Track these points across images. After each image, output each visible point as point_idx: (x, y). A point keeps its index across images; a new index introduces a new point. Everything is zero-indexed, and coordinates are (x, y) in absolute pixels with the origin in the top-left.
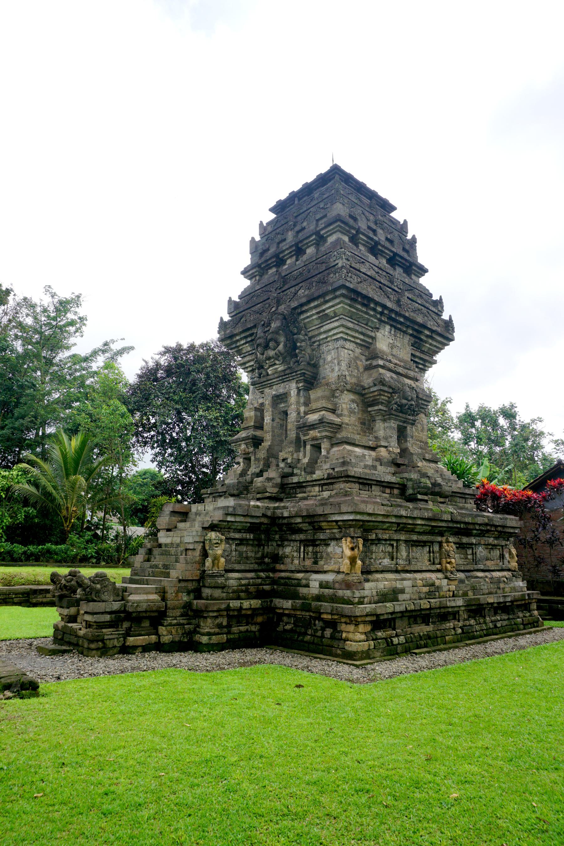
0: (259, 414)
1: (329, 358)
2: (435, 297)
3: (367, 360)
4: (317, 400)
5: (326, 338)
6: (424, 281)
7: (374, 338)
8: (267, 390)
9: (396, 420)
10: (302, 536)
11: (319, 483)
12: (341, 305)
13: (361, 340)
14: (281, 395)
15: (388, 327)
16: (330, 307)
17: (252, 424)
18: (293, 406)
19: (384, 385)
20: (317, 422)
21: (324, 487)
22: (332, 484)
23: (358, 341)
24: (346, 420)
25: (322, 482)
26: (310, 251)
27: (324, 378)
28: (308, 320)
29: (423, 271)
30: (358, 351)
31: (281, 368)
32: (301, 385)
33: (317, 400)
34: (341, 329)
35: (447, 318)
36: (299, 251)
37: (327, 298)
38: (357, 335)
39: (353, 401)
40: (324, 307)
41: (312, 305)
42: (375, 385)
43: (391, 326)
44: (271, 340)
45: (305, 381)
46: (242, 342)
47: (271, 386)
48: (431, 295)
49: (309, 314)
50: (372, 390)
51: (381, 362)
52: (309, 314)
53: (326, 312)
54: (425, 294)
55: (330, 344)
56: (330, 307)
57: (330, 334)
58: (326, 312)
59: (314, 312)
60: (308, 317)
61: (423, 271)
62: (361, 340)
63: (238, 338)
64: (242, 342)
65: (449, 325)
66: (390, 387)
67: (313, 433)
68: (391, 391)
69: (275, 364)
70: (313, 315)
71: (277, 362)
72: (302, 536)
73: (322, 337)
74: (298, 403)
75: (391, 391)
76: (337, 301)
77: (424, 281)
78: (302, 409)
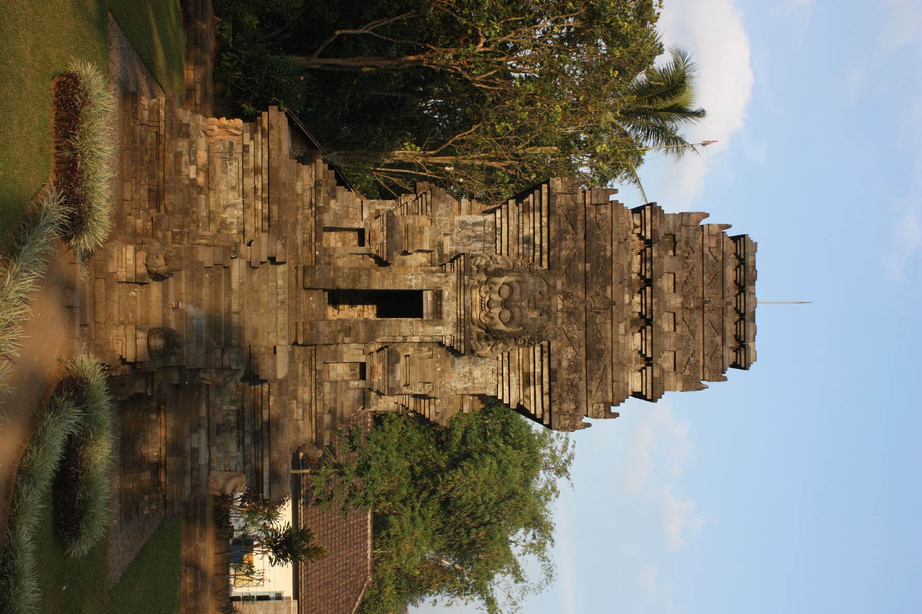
1: (477, 373)
5: (502, 374)
14: (441, 305)
26: (635, 341)
27: (453, 363)
28: (531, 355)
31: (475, 315)
37: (546, 398)
53: (532, 388)
55: (495, 376)
57: (506, 384)
58: (532, 388)
59: (538, 370)
63: (545, 219)
64: (537, 225)
71: (483, 314)
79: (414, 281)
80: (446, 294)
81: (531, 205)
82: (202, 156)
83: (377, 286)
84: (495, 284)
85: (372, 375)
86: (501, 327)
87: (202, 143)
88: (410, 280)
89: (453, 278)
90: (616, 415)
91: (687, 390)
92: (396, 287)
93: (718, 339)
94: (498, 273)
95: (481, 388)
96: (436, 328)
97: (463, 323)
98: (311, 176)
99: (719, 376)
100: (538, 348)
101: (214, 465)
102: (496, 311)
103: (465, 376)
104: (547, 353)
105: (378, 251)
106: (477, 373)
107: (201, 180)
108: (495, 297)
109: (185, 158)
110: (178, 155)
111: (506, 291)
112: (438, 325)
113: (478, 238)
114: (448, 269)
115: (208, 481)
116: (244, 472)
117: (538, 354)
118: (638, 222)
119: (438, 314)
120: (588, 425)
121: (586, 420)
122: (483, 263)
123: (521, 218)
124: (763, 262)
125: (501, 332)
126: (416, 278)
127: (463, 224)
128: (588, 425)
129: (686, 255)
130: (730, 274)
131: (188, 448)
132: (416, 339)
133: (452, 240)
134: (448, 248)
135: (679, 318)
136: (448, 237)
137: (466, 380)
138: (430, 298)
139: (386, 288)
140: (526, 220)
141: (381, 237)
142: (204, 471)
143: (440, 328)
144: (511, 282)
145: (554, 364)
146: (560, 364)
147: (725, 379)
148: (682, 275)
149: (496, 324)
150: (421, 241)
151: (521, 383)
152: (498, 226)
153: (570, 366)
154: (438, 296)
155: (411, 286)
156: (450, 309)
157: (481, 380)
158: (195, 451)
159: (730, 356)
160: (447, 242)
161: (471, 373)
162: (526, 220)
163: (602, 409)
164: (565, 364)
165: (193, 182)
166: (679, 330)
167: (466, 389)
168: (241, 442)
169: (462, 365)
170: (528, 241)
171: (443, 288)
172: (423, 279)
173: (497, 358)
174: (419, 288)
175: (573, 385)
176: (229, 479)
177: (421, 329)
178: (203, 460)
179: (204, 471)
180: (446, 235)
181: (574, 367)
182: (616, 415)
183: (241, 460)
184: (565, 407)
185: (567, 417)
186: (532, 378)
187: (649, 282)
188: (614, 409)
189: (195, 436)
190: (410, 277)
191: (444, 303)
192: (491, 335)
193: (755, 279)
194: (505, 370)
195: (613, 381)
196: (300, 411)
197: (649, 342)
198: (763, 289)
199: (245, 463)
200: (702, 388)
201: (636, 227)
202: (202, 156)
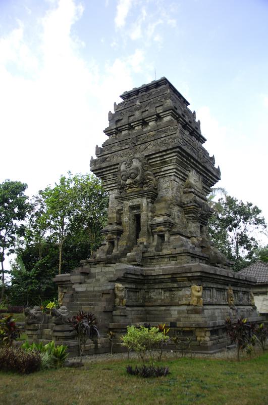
0: (118, 216)
2: (211, 156)
3: (184, 188)
4: (161, 209)
5: (164, 174)
6: (204, 145)
7: (187, 176)
8: (125, 202)
9: (199, 222)
12: (176, 157)
13: (182, 177)
15: (194, 171)
17: (116, 222)
18: (144, 212)
19: (196, 203)
21: (171, 259)
23: (181, 177)
24: (177, 221)
25: (170, 256)
27: (162, 197)
28: (154, 163)
29: (204, 140)
30: (180, 183)
33: (161, 209)
34: (175, 170)
35: (217, 167)
36: (144, 123)
38: (181, 174)
39: (179, 210)
40: (165, 157)
42: (191, 202)
43: (196, 170)
45: (152, 198)
48: (208, 154)
50: (189, 205)
51: (193, 190)
54: (205, 153)
59: (158, 159)
61: (204, 140)
62: (182, 177)
65: (218, 171)
66: (198, 204)
67: (159, 228)
68: (198, 206)
69: (133, 187)
70: (158, 161)
71: (134, 186)
73: (162, 173)
74: (147, 210)
75: (198, 206)
76: (174, 154)
77: (204, 145)
78: (150, 214)
80: (131, 204)
85: (162, 231)
97: (141, 195)
103: (167, 191)
106: (165, 186)
119: (138, 207)
124: (129, 88)
125: (141, 177)
138: (135, 211)
151: (167, 165)
154: (132, 208)
156: (136, 201)
162: (106, 178)
172: (126, 215)
173: (158, 178)
191: (134, 204)
194: (162, 173)
197: (151, 118)
198: (138, 85)
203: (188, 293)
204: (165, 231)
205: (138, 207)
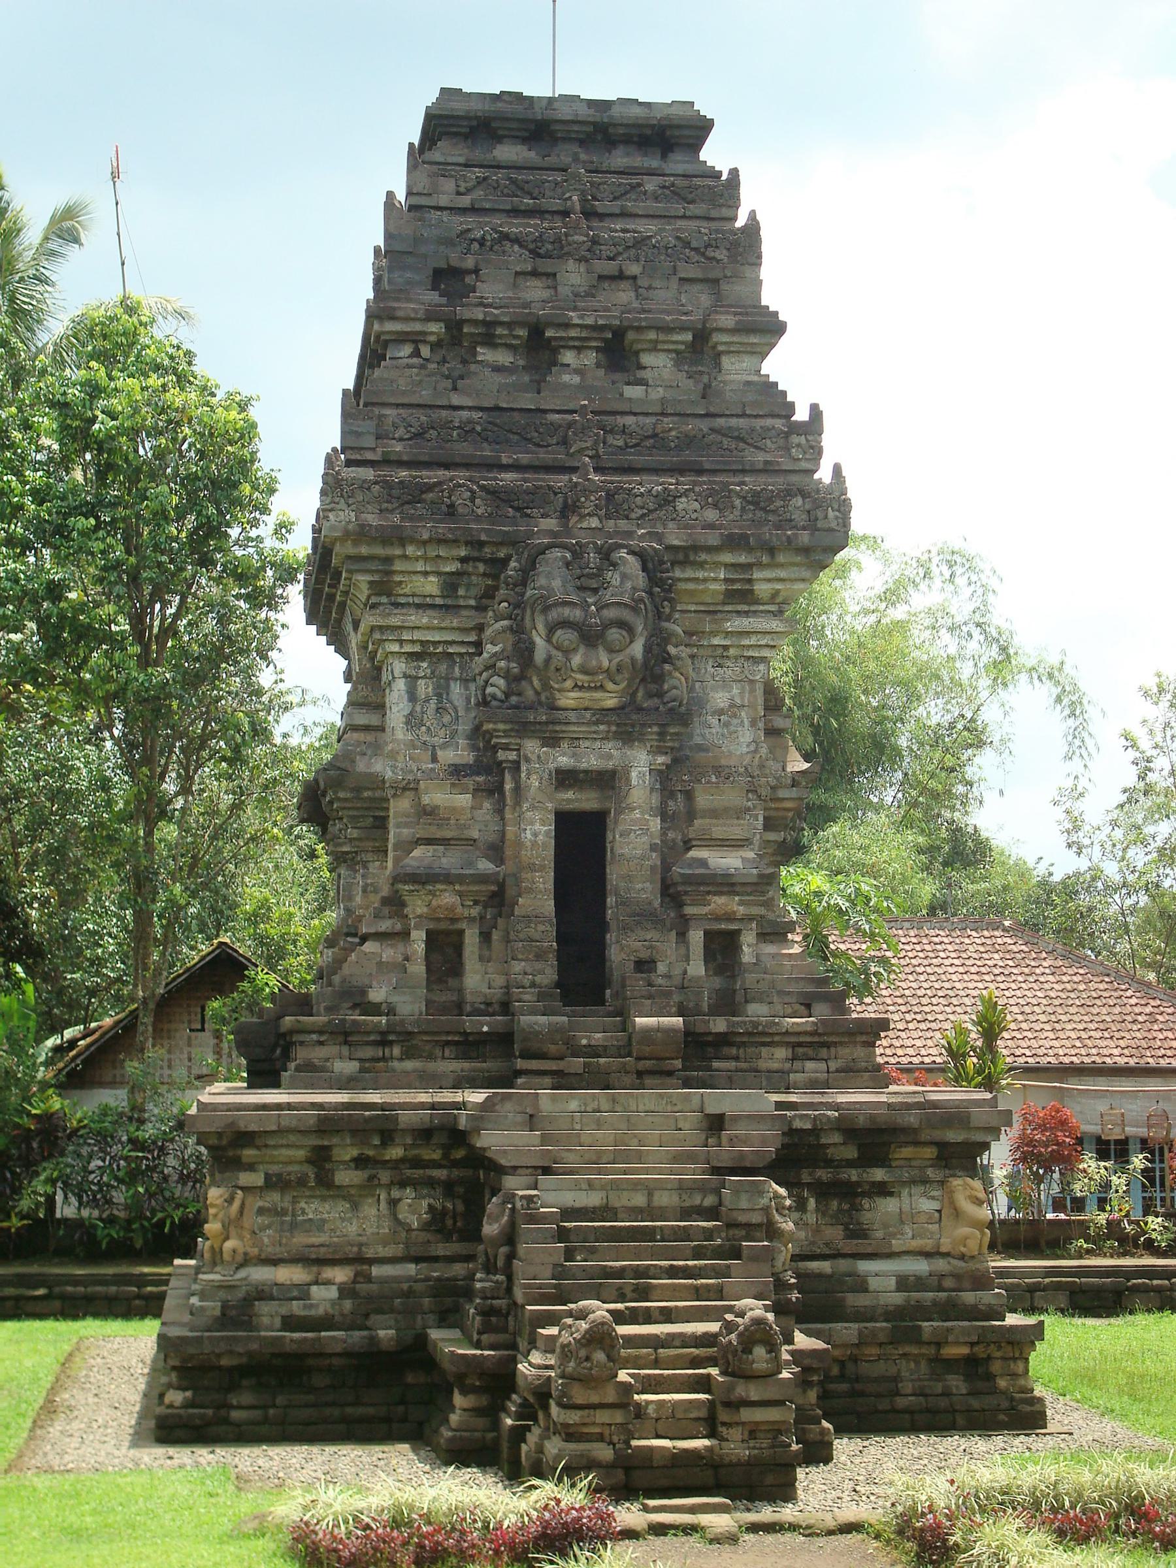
1: (720, 699)
5: (726, 648)
10: (823, 1174)
11: (787, 1039)
14: (586, 772)
16: (769, 580)
20: (755, 880)
22: (827, 1045)
27: (700, 748)
32: (661, 759)
36: (618, 350)
41: (727, 558)
44: (622, 624)
46: (420, 566)
47: (552, 741)
49: (701, 574)
52: (701, 574)
56: (769, 580)
57: (746, 642)
60: (696, 580)
64: (420, 566)
67: (719, 902)
69: (602, 687)
71: (610, 686)
72: (823, 1174)
79: (537, 827)
80: (564, 761)
81: (376, 578)
82: (286, 1274)
83: (549, 906)
84: (548, 660)
85: (730, 917)
86: (637, 649)
87: (260, 1274)
88: (535, 835)
89: (531, 746)
90: (816, 412)
91: (760, 257)
92: (550, 864)
93: (651, 184)
94: (523, 652)
95: (752, 691)
96: (634, 782)
97: (625, 725)
98: (321, 1043)
99: (726, 189)
100: (678, 573)
101: (927, 1244)
102: (604, 659)
103: (727, 725)
104: (685, 556)
105: (476, 903)
106: (720, 699)
107: (340, 1275)
108: (577, 660)
109: (296, 1308)
110: (290, 1323)
111: (564, 636)
112: (628, 780)
113: (441, 692)
114: (512, 756)
115: (962, 1257)
116: (942, 1183)
117: (689, 573)
118: (407, 350)
119: (607, 781)
120: (837, 470)
121: (824, 474)
122: (501, 682)
123: (402, 600)
124: (485, 78)
125: (647, 649)
126: (532, 824)
127: (412, 721)
128: (837, 470)
129: (476, 246)
130: (508, 152)
131: (898, 1298)
132: (655, 824)
133: (444, 746)
134: (460, 753)
135: (610, 268)
136: (439, 753)
137: (735, 721)
139: (550, 885)
140: (407, 591)
141: (448, 898)
142: (941, 1265)
143: (634, 774)
144: (547, 624)
145: (713, 539)
146: (711, 526)
147: (734, 172)
148: (518, 258)
149: (633, 659)
150: (454, 809)
151: (746, 608)
152: (417, 648)
153: (715, 506)
155: (547, 833)
157: (735, 691)
158: (904, 1283)
159: (677, 164)
160: (448, 756)
161: (721, 712)
163: (802, 440)
164: (711, 515)
165: (346, 1291)
166: (634, 269)
167: (753, 723)
168: (882, 1190)
169: (708, 730)
170: (451, 584)
171: (552, 766)
172: (533, 808)
174: (552, 817)
175: (755, 500)
176: (957, 1213)
177: (637, 814)
178: (921, 1267)
179: (941, 1265)
180: (434, 759)
181: (718, 499)
182: (816, 412)
183: (917, 1190)
184: (800, 518)
185: (820, 514)
186: (737, 586)
187: (536, 331)
188: (802, 415)
189: (873, 1283)
190: (529, 836)
192: (653, 670)
193: (518, 96)
195: (744, 415)
196: (810, 1065)
197: (662, 337)
199: (925, 1181)
200: (753, 229)
201: (416, 353)
202: (286, 1274)
203: (928, 1206)
204: (750, 918)
205: (607, 781)
